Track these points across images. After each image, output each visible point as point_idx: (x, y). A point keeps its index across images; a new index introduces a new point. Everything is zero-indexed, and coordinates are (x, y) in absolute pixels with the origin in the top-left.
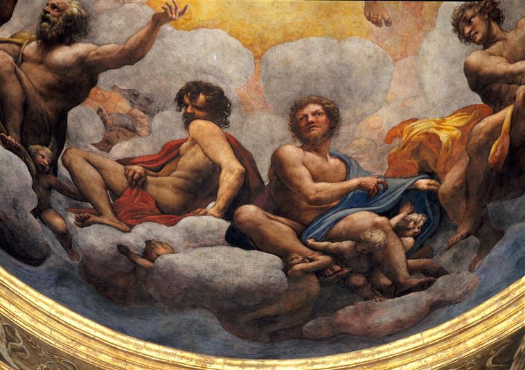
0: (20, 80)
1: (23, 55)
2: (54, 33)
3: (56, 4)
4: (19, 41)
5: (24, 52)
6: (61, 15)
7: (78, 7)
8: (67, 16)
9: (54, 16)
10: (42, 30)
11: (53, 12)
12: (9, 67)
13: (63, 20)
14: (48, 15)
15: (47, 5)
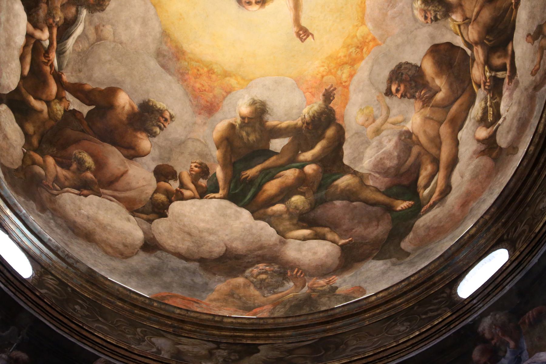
0: (478, 14)
1: (464, 21)
2: (440, 7)
3: (423, 17)
4: (457, 28)
5: (461, 20)
6: (427, 10)
7: (416, 2)
8: (426, 5)
9: (431, 14)
10: (443, 17)
11: (429, 15)
12: (475, 26)
13: (429, 6)
14: (433, 18)
15: (427, 23)
